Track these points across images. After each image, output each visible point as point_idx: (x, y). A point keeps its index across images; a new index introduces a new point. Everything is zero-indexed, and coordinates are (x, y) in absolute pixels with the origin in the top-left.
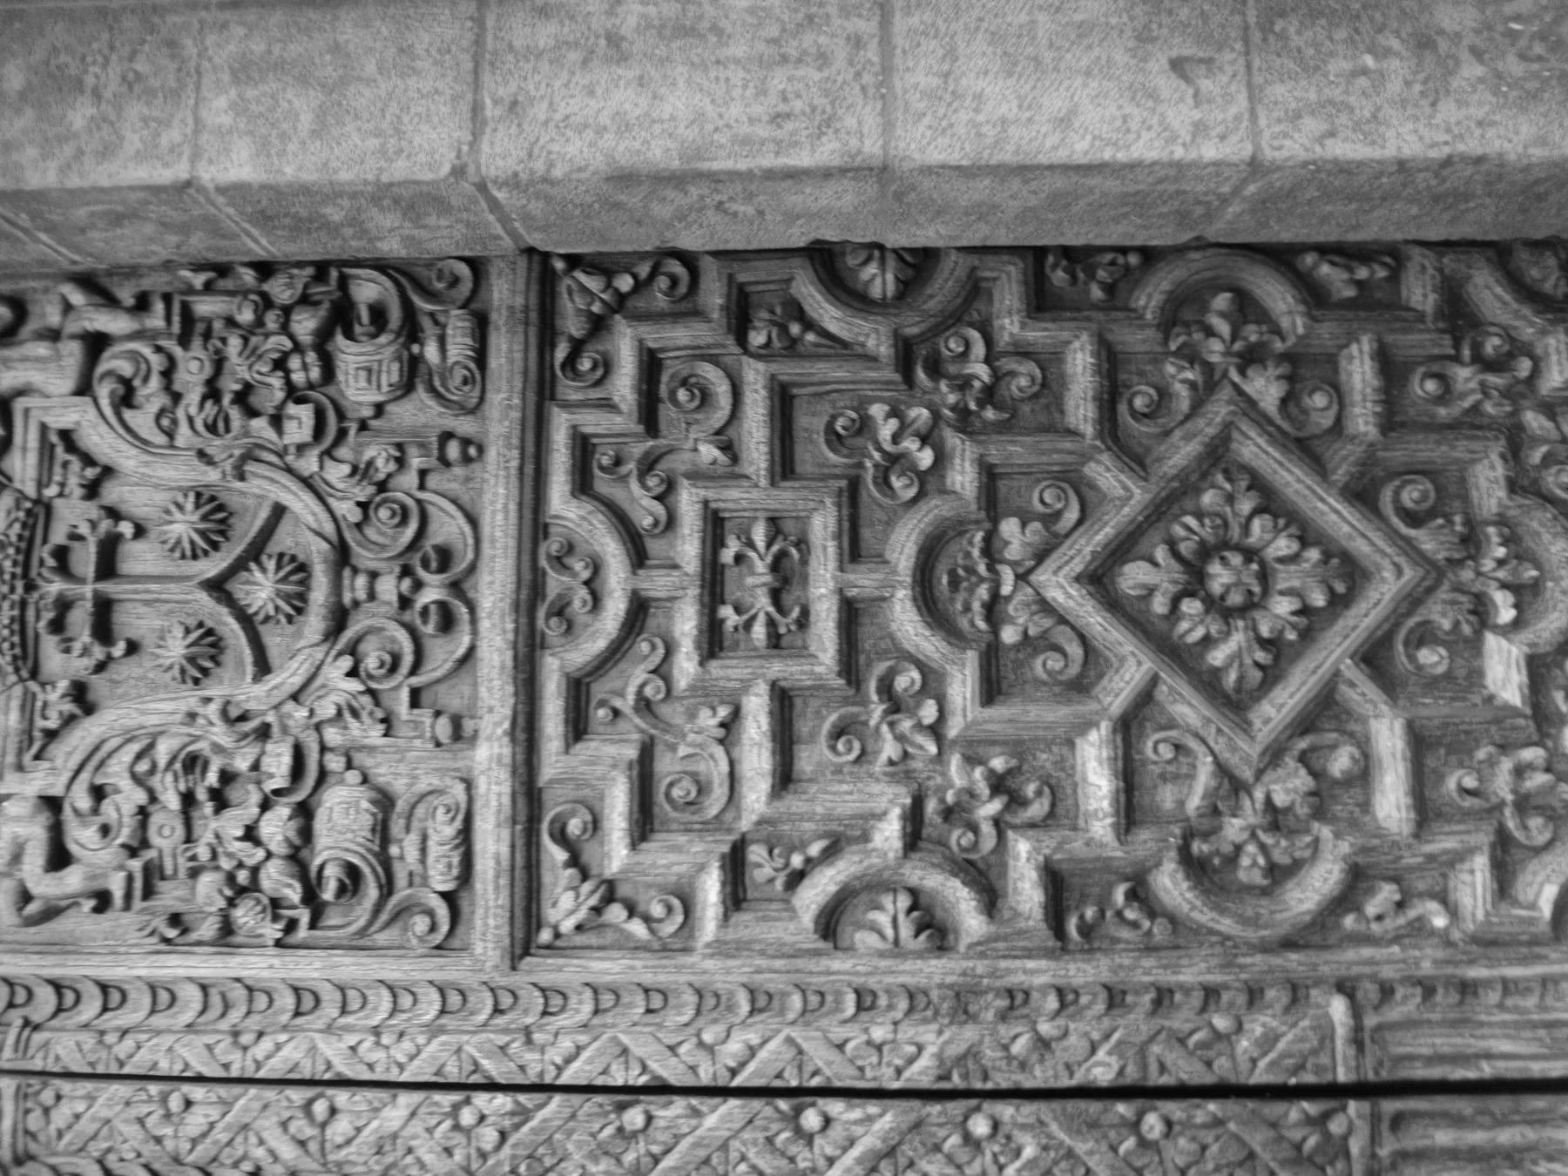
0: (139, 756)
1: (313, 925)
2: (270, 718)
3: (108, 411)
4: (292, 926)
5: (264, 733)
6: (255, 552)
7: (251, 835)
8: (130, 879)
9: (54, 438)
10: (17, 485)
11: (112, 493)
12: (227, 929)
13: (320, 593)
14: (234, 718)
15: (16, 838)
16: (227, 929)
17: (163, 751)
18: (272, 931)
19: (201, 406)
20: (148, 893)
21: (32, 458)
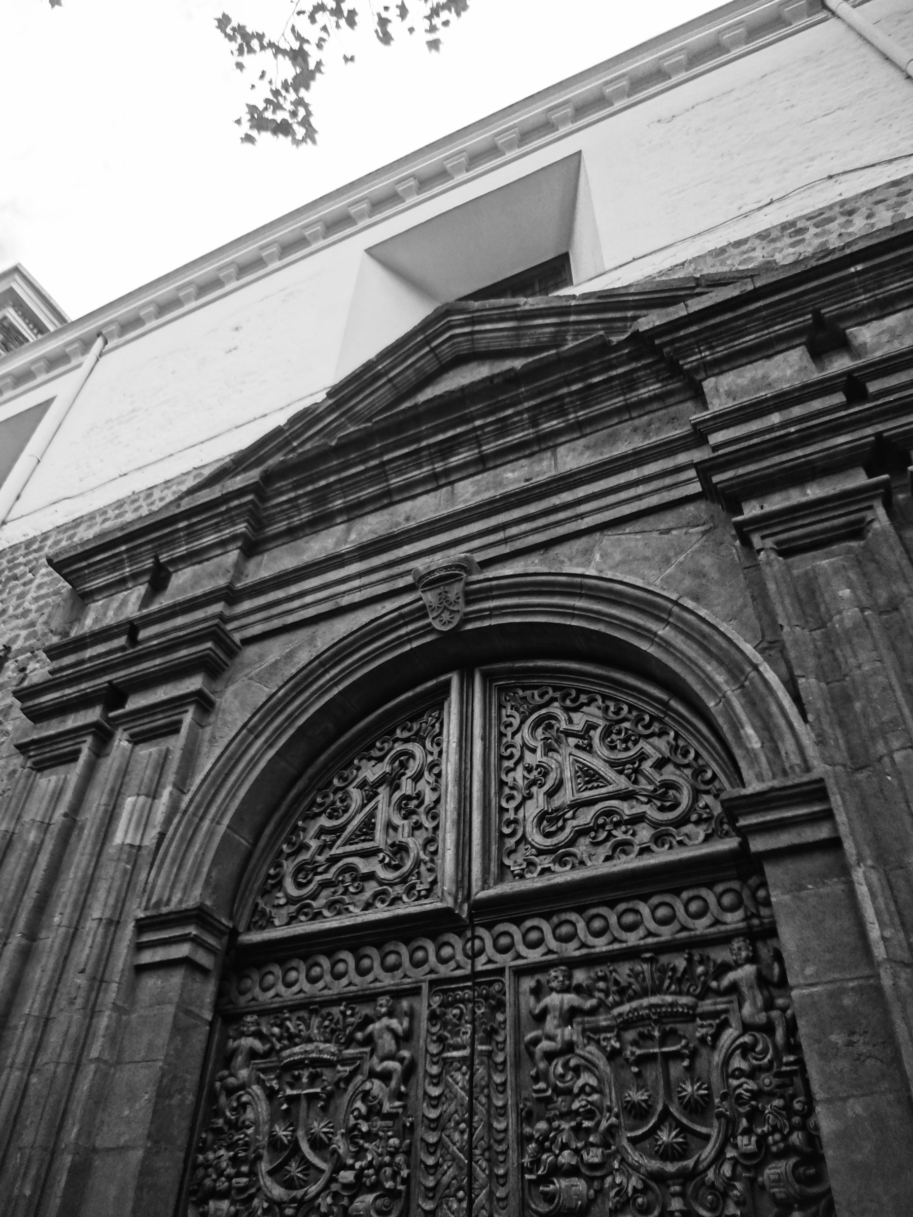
0: (591, 1087)
1: (530, 1181)
2: (613, 1148)
3: (738, 1042)
4: (531, 1172)
5: (606, 1145)
6: (684, 1130)
7: (564, 1146)
8: (545, 1091)
9: (723, 1017)
10: (700, 1003)
11: (704, 1051)
12: (530, 1139)
13: (670, 1168)
14: (612, 1131)
15: (556, 1036)
16: (530, 1139)
17: (595, 1097)
18: (526, 1160)
19: (747, 1090)
20: (539, 1100)
21: (712, 1008)
